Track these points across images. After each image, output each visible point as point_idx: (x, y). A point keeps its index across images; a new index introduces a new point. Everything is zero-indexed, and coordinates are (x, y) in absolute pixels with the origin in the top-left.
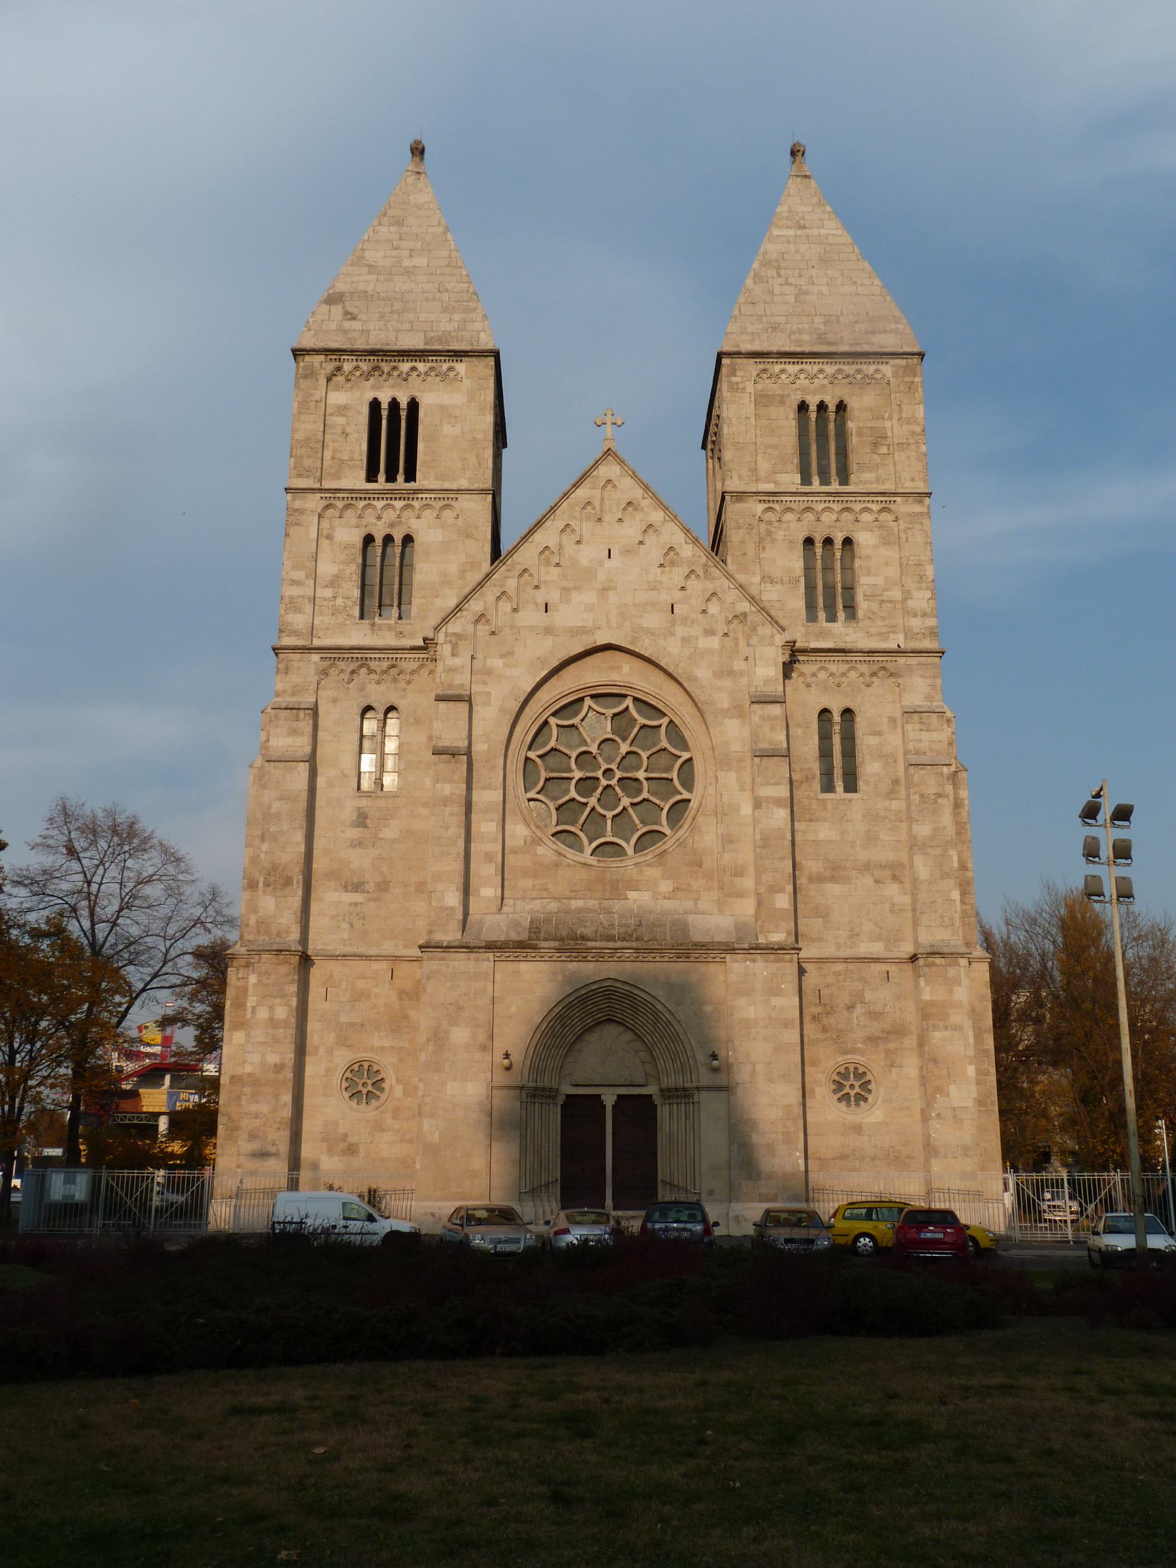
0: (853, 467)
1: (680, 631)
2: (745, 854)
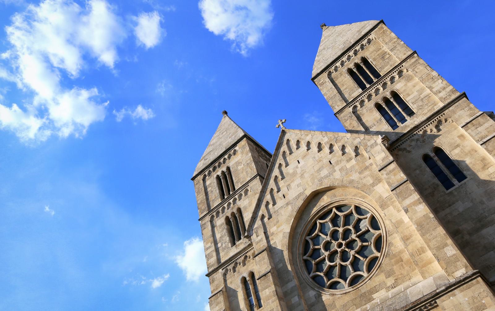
1: (337, 168)
2: (418, 240)
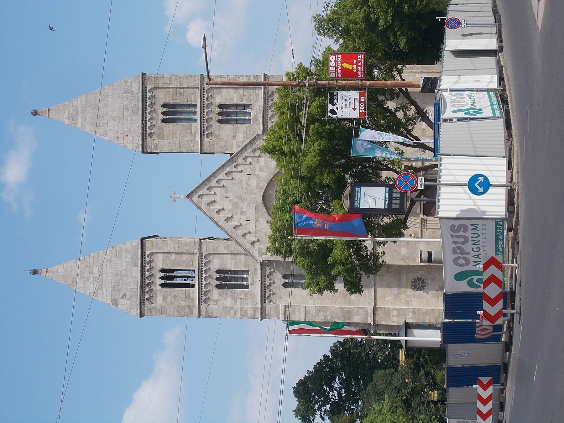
0: (189, 103)
1: (257, 172)
